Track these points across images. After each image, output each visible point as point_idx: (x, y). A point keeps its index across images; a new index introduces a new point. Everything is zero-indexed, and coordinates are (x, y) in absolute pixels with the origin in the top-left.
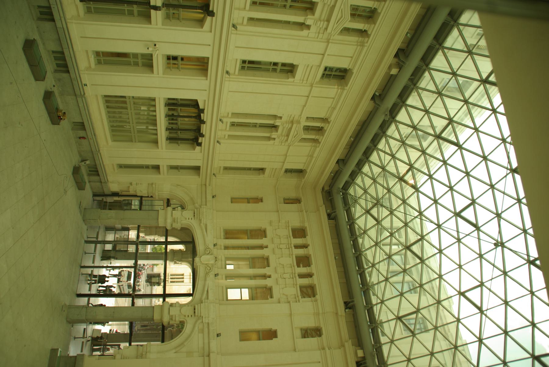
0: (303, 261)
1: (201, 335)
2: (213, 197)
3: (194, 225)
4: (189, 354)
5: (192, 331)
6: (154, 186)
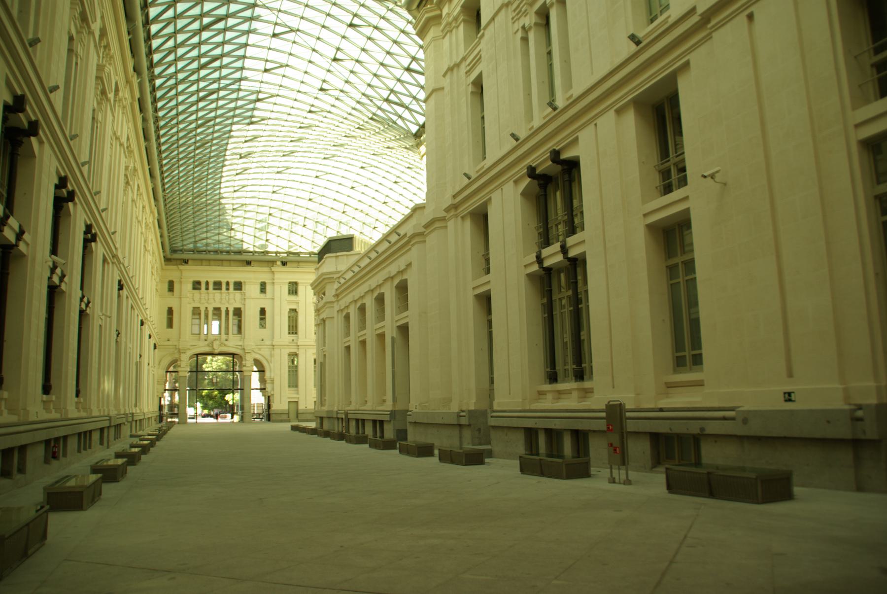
0: (218, 285)
1: (262, 350)
2: (168, 340)
3: (190, 353)
4: (271, 355)
5: (260, 354)
6: (159, 380)
